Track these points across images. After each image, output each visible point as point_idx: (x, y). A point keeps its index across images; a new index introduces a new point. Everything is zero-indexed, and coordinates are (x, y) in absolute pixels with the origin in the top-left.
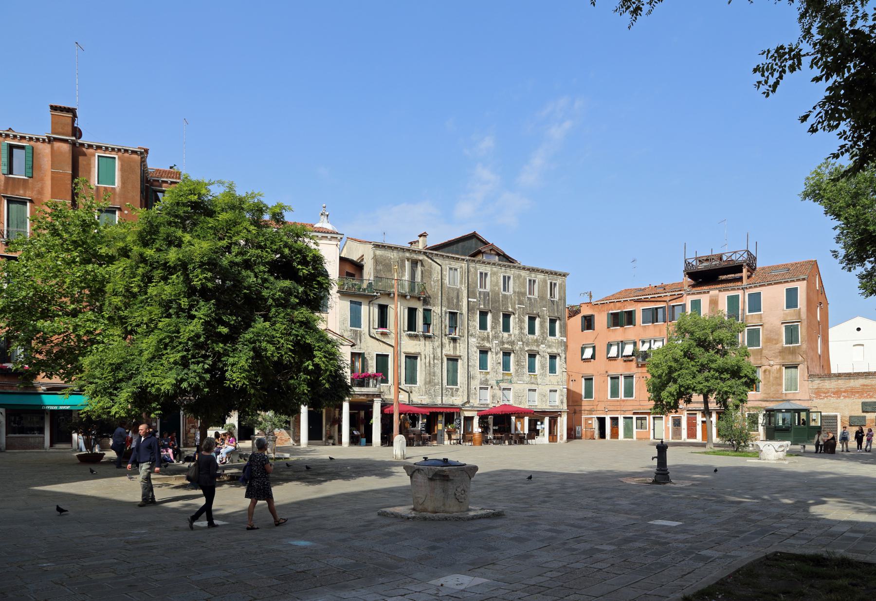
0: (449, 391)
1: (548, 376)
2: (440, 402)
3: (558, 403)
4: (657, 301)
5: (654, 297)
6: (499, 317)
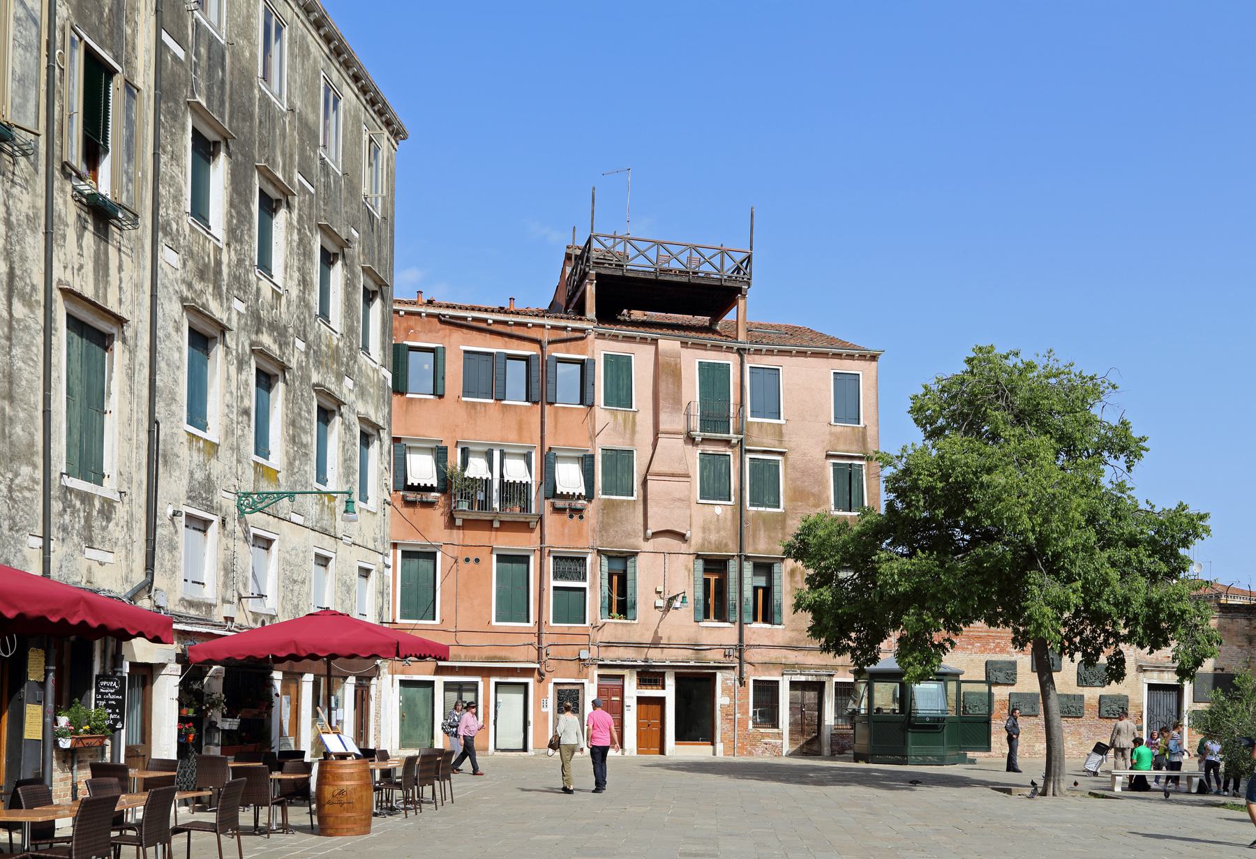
0: (75, 512)
2: (36, 569)
4: (511, 336)
5: (505, 323)
6: (251, 200)
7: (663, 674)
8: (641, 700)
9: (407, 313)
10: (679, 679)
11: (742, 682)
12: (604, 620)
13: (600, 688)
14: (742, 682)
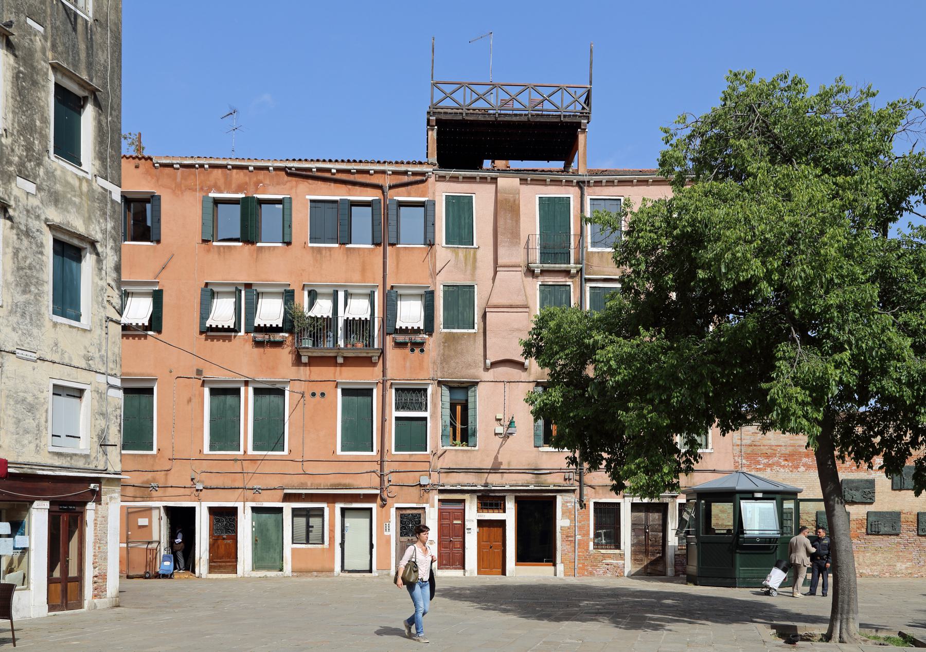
1: (48, 325)
3: (85, 445)
4: (354, 184)
5: (348, 171)
7: (503, 498)
8: (481, 523)
9: (256, 168)
10: (519, 502)
11: (583, 505)
12: (445, 448)
13: (441, 512)
14: (583, 505)
